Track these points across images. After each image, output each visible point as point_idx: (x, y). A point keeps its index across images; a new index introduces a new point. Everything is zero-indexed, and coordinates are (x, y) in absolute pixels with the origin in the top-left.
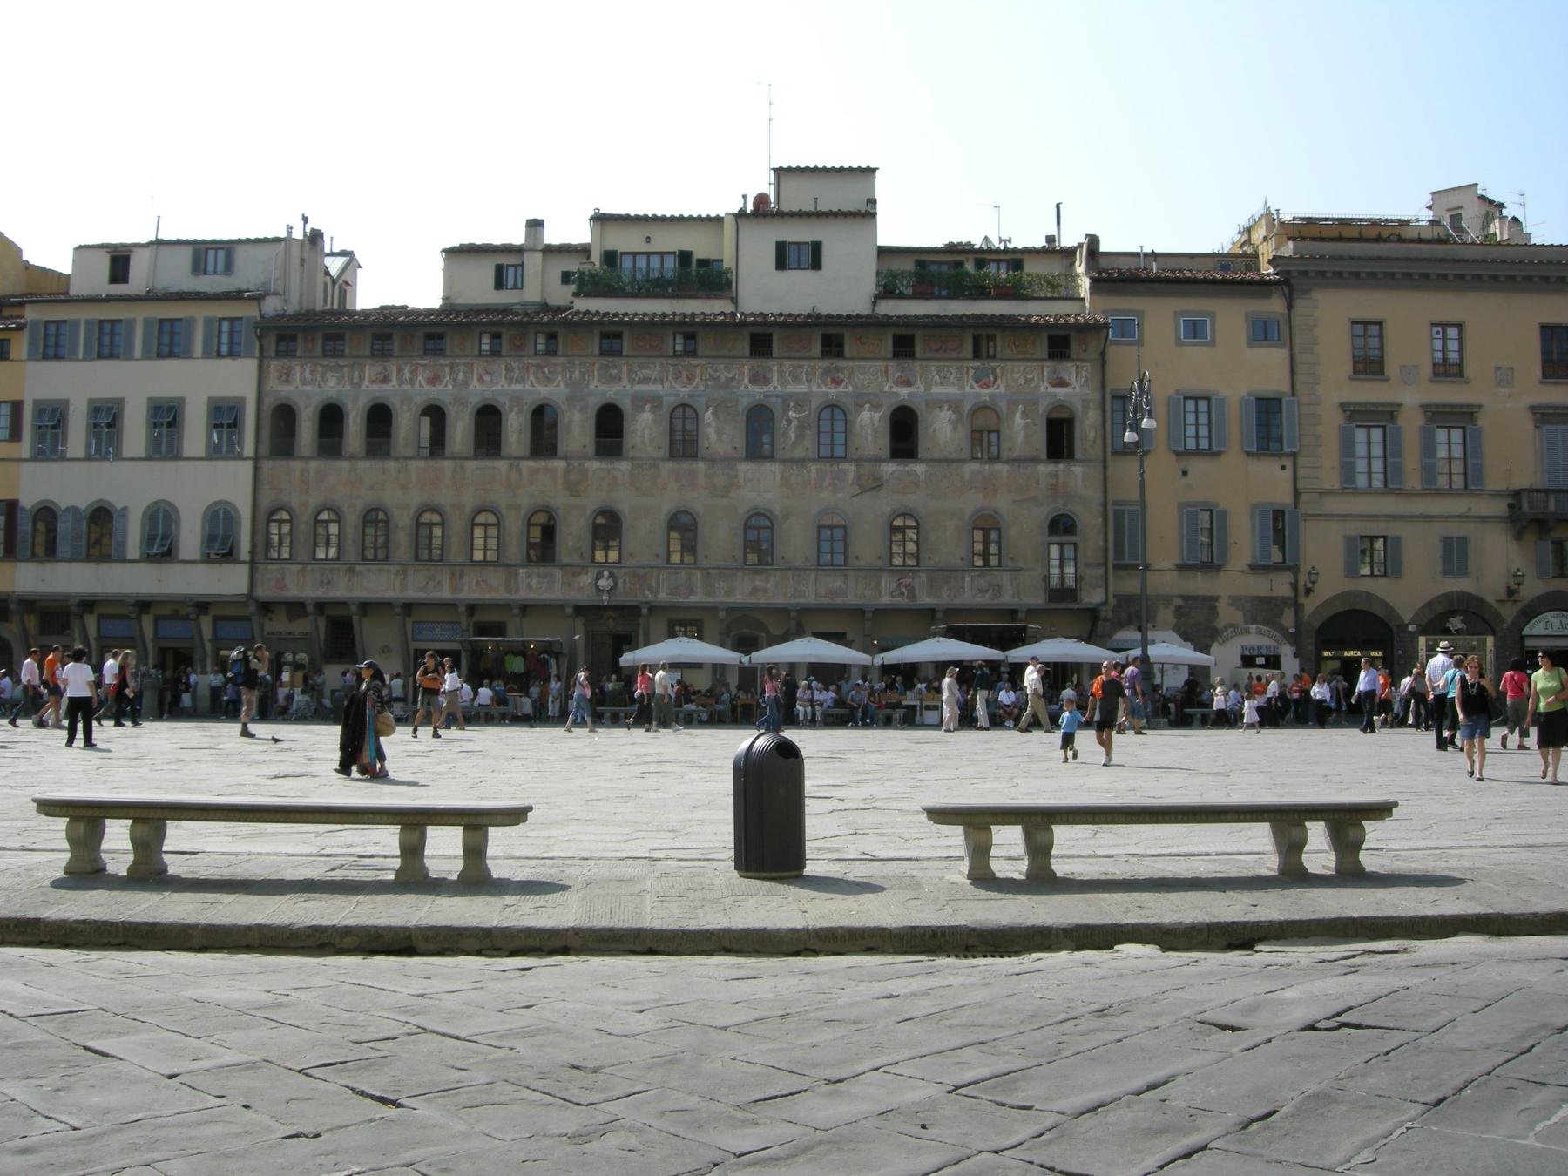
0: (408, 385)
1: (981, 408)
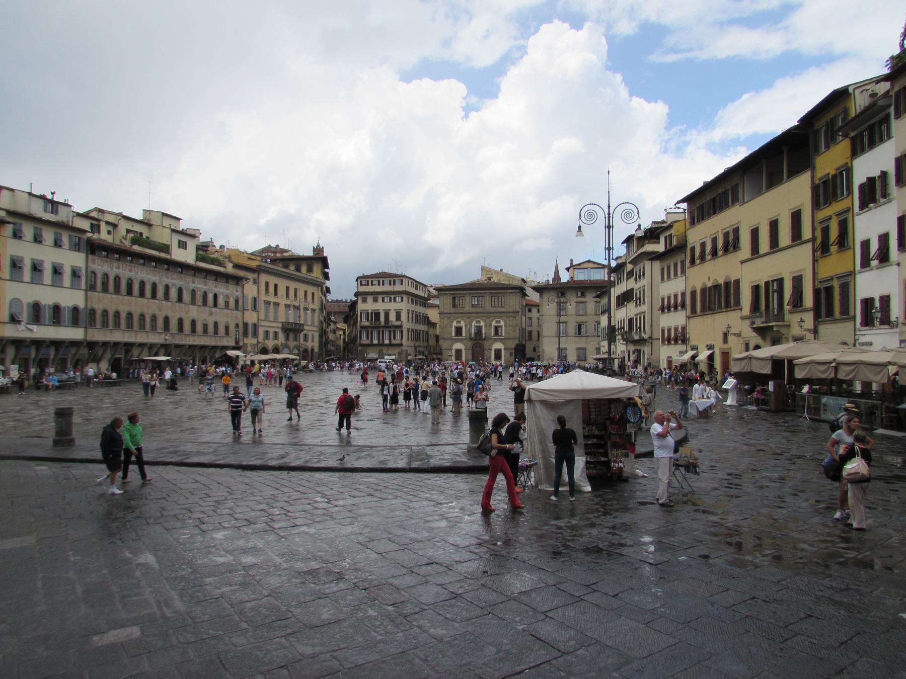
0: (175, 280)
1: (227, 296)
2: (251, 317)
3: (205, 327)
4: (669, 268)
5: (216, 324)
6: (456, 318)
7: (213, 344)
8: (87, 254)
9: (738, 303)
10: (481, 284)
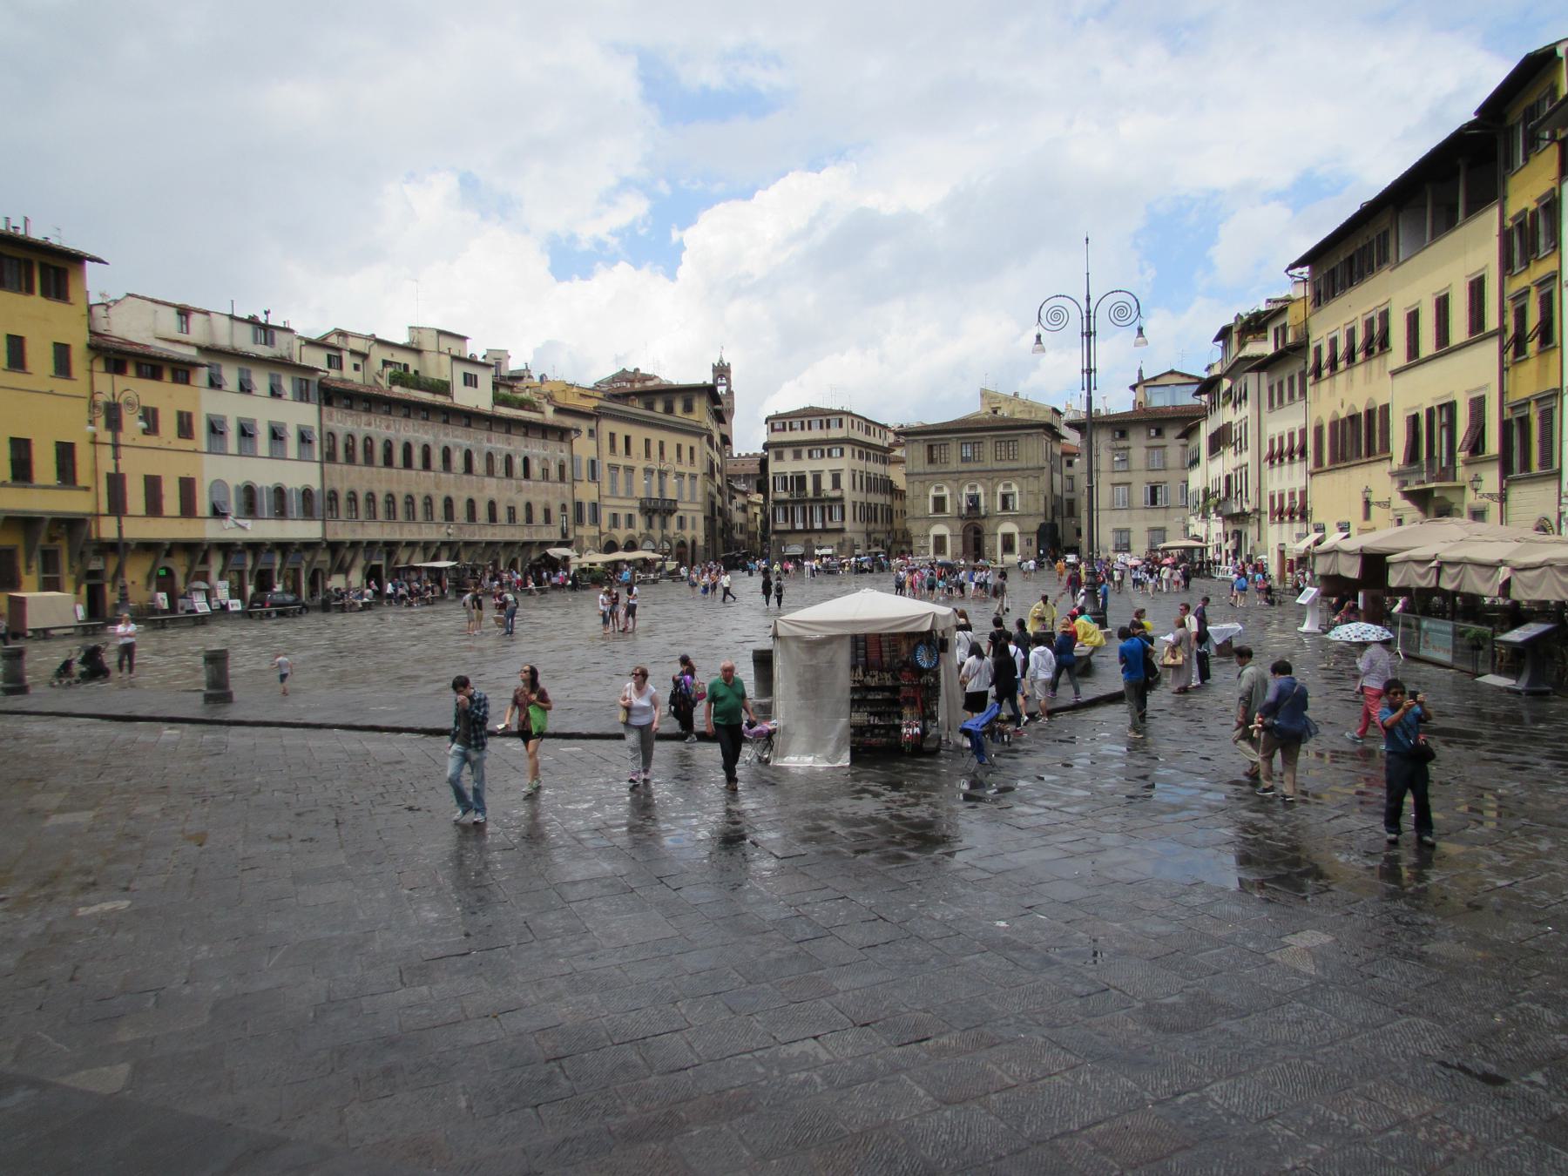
0: (458, 439)
2: (587, 492)
3: (511, 511)
4: (1281, 384)
5: (529, 506)
6: (934, 481)
7: (526, 538)
8: (320, 405)
9: (1386, 447)
10: (978, 421)
